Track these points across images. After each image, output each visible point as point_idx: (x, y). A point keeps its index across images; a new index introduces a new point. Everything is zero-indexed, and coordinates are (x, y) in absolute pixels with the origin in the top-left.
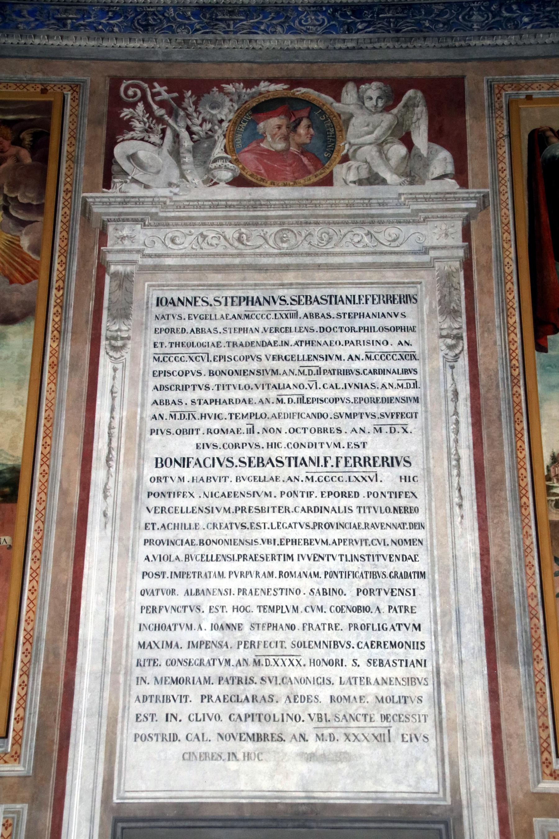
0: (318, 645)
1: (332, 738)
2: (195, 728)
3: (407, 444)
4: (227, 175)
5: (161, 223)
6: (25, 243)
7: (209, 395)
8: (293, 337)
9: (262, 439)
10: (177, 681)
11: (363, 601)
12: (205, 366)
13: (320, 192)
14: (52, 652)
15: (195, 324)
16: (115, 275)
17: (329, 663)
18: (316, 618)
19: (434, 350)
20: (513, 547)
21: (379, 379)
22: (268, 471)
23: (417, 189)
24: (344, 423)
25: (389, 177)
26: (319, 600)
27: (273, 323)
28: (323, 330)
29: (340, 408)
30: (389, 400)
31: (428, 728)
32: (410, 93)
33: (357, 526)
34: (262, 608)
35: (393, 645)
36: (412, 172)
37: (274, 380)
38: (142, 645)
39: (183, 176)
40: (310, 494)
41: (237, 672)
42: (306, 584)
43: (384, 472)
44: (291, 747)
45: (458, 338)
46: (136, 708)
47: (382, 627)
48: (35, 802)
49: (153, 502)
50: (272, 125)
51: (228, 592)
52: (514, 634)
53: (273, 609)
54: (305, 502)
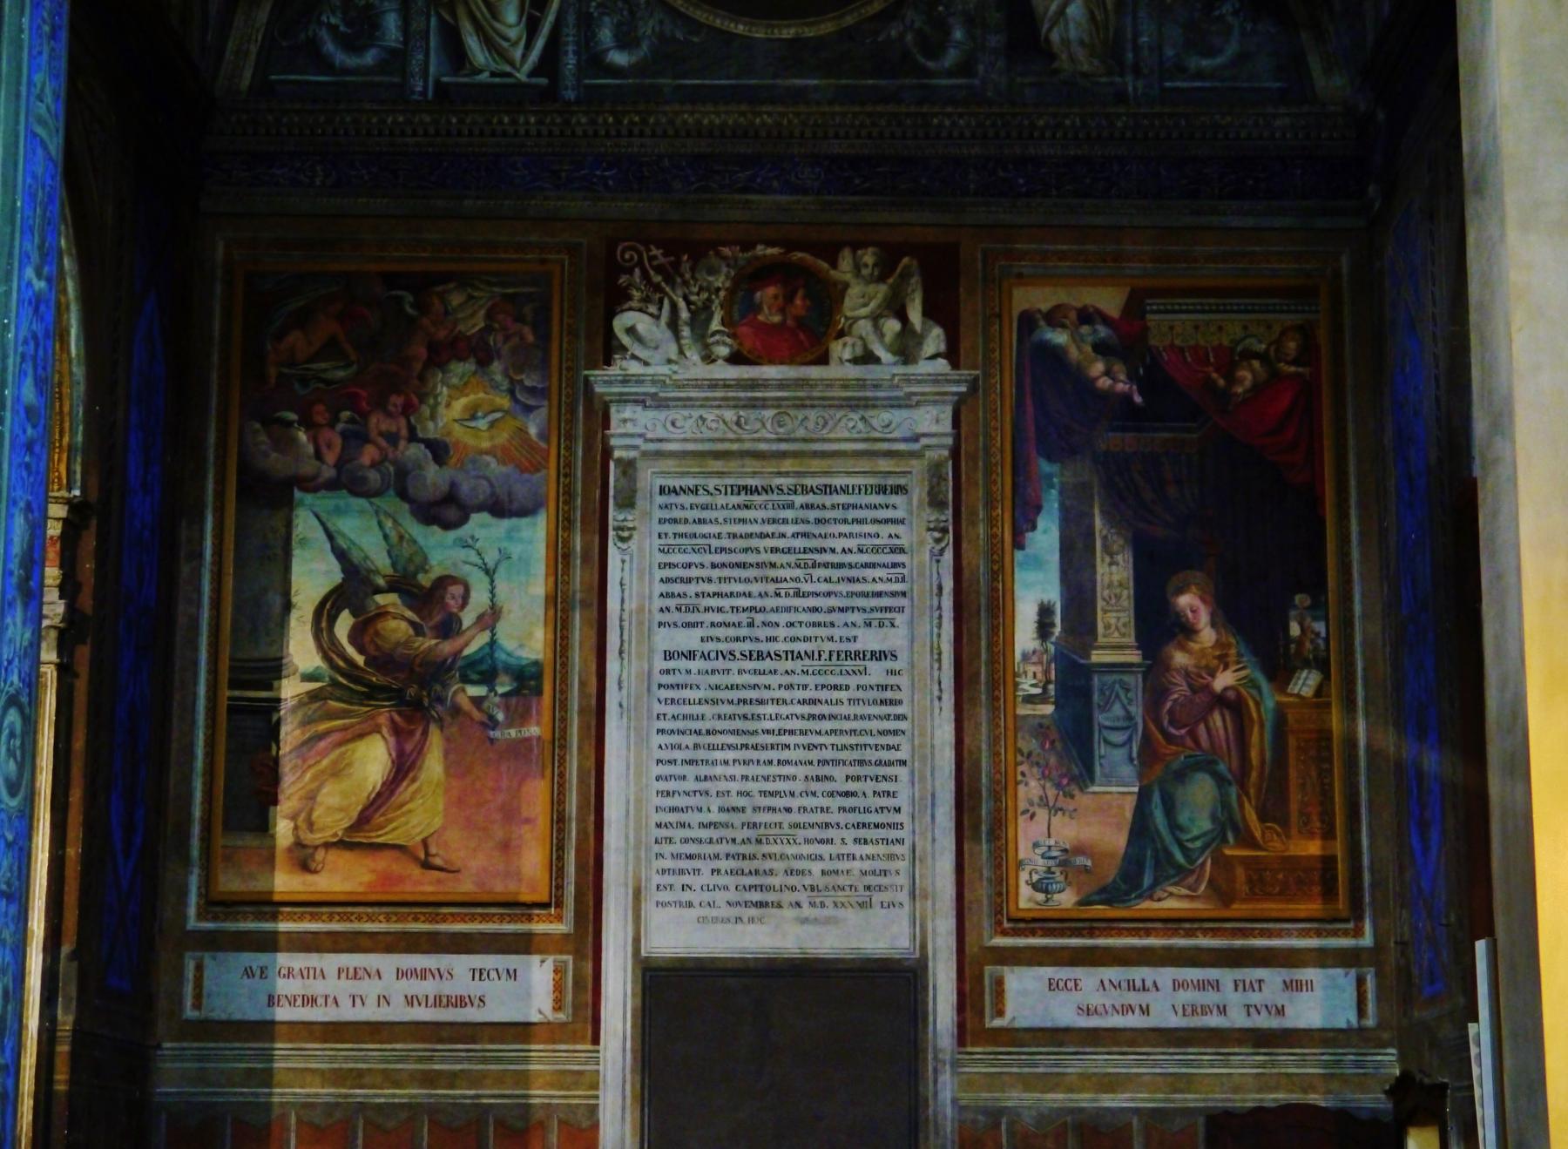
0: (812, 826)
1: (823, 905)
2: (707, 896)
3: (895, 639)
4: (723, 351)
5: (661, 403)
6: (533, 431)
7: (711, 588)
8: (790, 529)
9: (762, 633)
10: (690, 857)
11: (852, 786)
12: (708, 558)
13: (815, 372)
14: (582, 833)
15: (697, 514)
16: (619, 461)
17: (821, 842)
18: (810, 802)
19: (922, 543)
20: (984, 738)
21: (869, 573)
22: (767, 664)
23: (910, 369)
24: (837, 617)
25: (881, 352)
26: (814, 786)
27: (771, 514)
28: (818, 521)
29: (833, 602)
30: (879, 594)
31: (903, 896)
32: (906, 260)
33: (847, 718)
34: (763, 793)
35: (876, 826)
36: (906, 349)
37: (772, 573)
38: (659, 826)
39: (681, 352)
40: (805, 687)
41: (743, 849)
42: (801, 771)
43: (873, 666)
44: (789, 913)
45: (944, 531)
46: (657, 879)
47: (867, 810)
48: (579, 955)
49: (664, 694)
50: (768, 294)
51: (733, 778)
52: (979, 816)
53: (772, 794)
54: (800, 694)
